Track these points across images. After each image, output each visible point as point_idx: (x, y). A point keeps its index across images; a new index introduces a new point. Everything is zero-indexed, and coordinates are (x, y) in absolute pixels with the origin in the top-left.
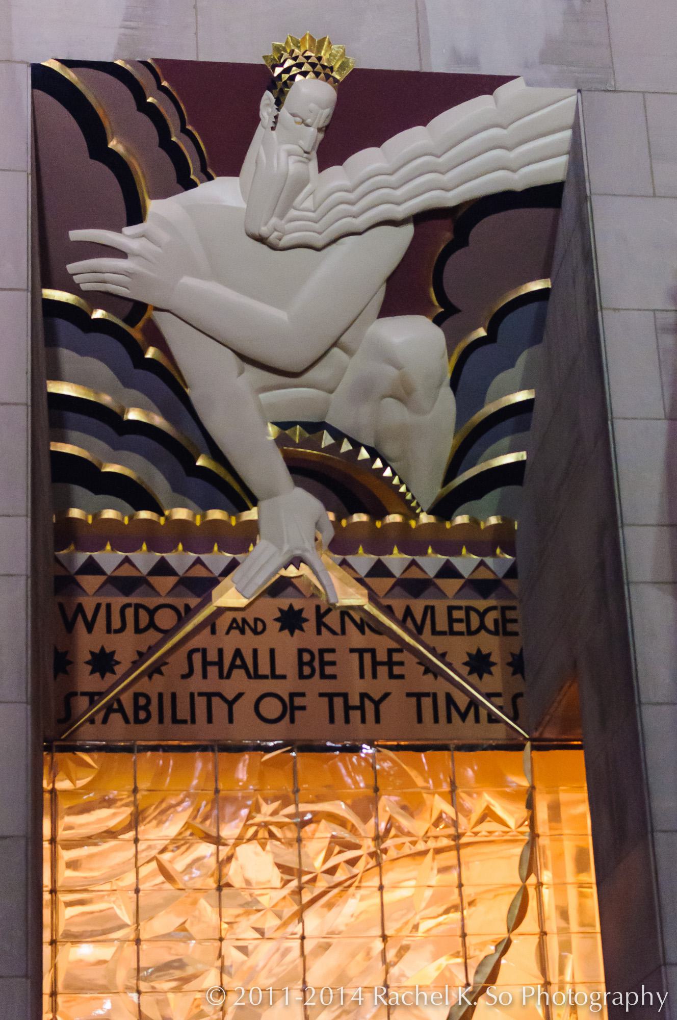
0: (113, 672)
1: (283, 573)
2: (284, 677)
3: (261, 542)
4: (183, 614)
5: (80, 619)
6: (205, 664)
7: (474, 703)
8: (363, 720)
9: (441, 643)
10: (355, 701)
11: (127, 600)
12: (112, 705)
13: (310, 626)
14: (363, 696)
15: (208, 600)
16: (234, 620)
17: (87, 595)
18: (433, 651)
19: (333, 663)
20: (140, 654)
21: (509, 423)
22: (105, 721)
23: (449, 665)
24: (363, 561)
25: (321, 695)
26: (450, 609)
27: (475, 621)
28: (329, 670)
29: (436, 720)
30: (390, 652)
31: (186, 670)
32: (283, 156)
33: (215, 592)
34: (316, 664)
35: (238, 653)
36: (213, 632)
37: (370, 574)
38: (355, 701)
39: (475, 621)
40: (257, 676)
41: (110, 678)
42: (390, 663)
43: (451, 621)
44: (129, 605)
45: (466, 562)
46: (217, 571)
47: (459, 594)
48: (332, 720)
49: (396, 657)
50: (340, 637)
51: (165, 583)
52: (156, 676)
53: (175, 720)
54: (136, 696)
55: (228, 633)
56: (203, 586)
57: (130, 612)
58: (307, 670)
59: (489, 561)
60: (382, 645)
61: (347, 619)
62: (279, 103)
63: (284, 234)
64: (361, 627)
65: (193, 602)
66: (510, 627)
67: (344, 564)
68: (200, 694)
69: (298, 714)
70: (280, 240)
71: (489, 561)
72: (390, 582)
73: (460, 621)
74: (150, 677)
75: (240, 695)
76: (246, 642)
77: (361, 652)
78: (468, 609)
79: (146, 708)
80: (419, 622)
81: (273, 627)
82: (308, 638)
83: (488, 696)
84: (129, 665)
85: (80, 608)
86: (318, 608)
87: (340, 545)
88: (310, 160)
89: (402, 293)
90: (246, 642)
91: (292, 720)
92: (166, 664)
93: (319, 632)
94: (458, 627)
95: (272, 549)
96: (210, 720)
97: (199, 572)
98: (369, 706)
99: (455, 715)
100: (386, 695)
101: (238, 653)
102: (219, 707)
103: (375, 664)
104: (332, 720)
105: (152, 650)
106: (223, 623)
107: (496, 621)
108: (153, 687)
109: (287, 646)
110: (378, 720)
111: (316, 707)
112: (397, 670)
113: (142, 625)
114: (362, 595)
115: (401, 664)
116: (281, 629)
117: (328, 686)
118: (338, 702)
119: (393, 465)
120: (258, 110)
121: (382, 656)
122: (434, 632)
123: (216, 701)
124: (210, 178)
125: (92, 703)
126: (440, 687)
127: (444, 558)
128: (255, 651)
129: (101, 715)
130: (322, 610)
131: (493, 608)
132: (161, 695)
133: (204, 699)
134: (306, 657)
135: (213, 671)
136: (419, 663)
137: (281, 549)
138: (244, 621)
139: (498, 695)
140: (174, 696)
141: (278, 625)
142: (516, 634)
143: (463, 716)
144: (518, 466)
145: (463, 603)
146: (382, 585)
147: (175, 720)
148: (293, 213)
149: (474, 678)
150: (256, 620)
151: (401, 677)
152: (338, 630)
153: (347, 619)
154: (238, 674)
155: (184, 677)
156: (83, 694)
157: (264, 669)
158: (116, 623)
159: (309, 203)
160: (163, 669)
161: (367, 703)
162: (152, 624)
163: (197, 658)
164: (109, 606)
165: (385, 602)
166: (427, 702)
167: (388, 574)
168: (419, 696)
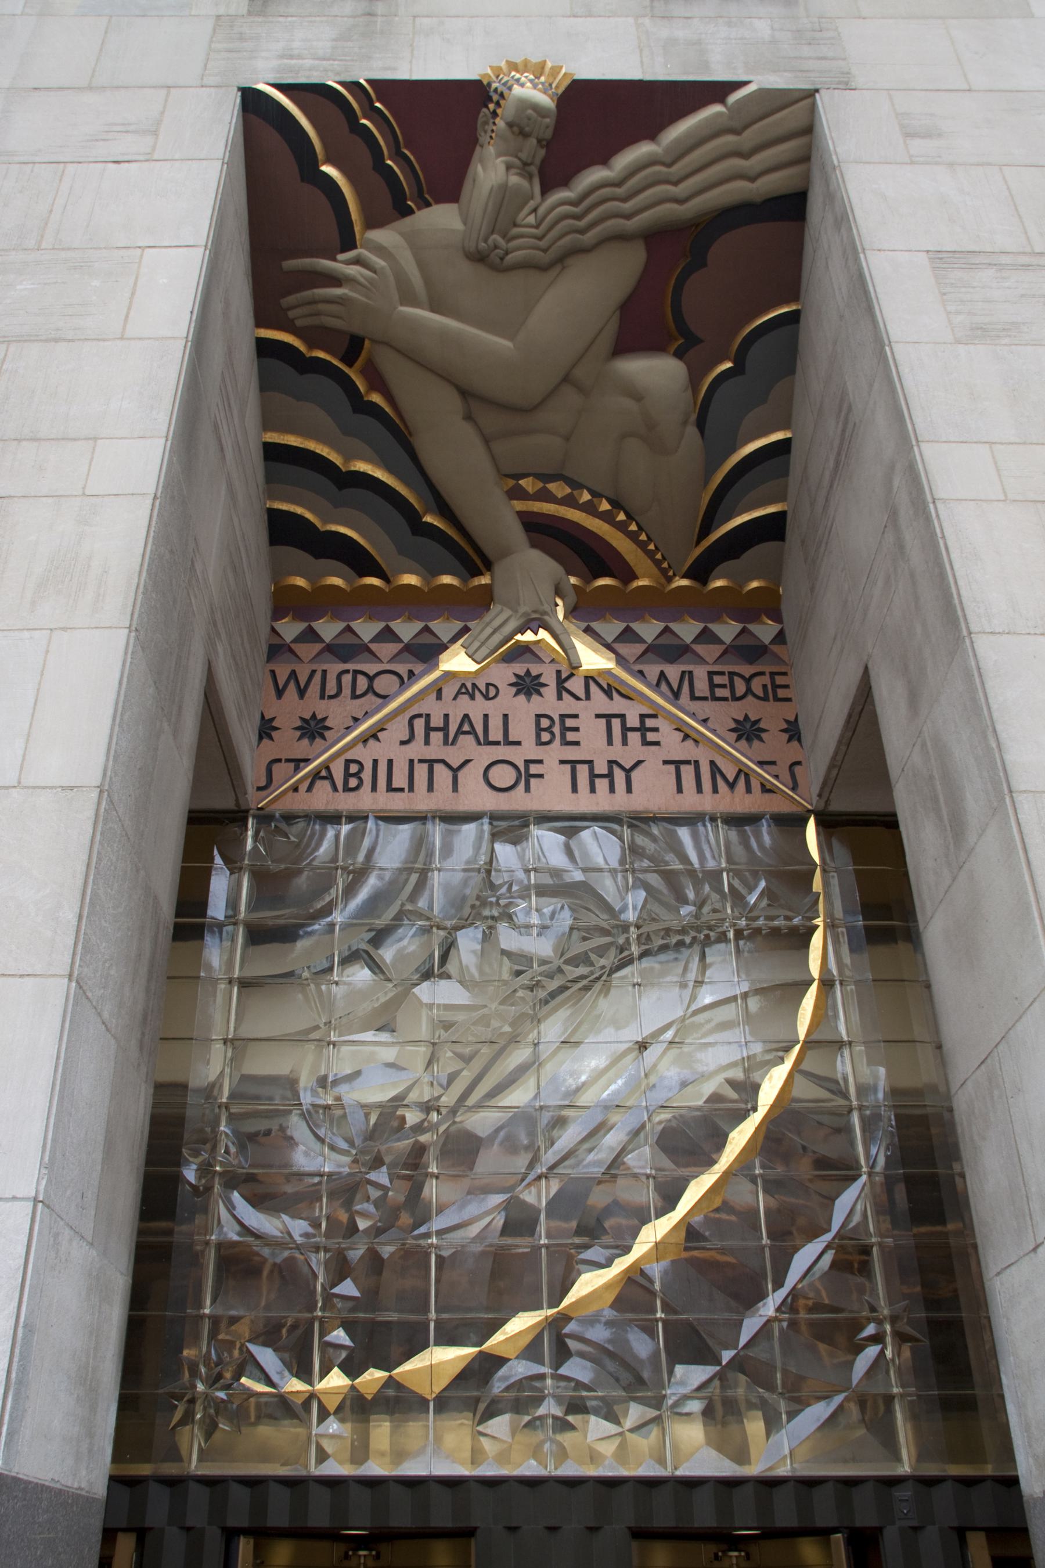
0: (324, 738)
2: (519, 743)
3: (495, 608)
4: (406, 680)
5: (292, 685)
6: (429, 729)
7: (742, 772)
8: (612, 789)
10: (601, 768)
12: (320, 772)
15: (437, 665)
16: (463, 685)
18: (693, 716)
19: (576, 729)
22: (309, 789)
23: (714, 731)
24: (611, 629)
25: (562, 762)
26: (711, 674)
27: (740, 687)
28: (571, 736)
29: (699, 789)
30: (643, 717)
32: (502, 168)
33: (443, 657)
34: (556, 730)
36: (439, 697)
37: (616, 640)
38: (601, 768)
39: (740, 687)
43: (712, 686)
44: (348, 671)
48: (575, 789)
49: (650, 723)
52: (371, 742)
53: (390, 789)
54: (348, 762)
55: (455, 699)
57: (347, 679)
58: (545, 737)
63: (507, 253)
64: (608, 692)
65: (418, 668)
67: (588, 630)
68: (421, 761)
69: (533, 781)
70: (502, 259)
72: (640, 648)
73: (723, 686)
74: (365, 741)
75: (467, 762)
77: (608, 717)
78: (732, 674)
79: (357, 775)
81: (507, 692)
82: (548, 702)
89: (641, 325)
90: (476, 708)
91: (527, 789)
92: (383, 729)
94: (720, 692)
95: (507, 613)
96: (430, 788)
98: (619, 776)
102: (442, 774)
103: (625, 729)
104: (575, 789)
105: (367, 715)
106: (449, 691)
107: (765, 686)
108: (365, 754)
109: (522, 713)
110: (629, 790)
111: (556, 777)
112: (651, 736)
113: (358, 692)
114: (609, 659)
115: (656, 730)
117: (572, 753)
118: (583, 771)
121: (633, 721)
122: (693, 697)
123: (438, 768)
124: (428, 205)
125: (297, 769)
128: (486, 716)
130: (564, 676)
131: (762, 674)
132: (375, 762)
133: (425, 766)
134: (545, 723)
135: (436, 737)
136: (677, 729)
137: (516, 611)
138: (474, 685)
139: (773, 763)
140: (390, 762)
141: (514, 690)
144: (781, 516)
146: (631, 651)
147: (390, 789)
148: (516, 231)
149: (743, 743)
150: (488, 685)
152: (582, 695)
154: (467, 740)
155: (403, 743)
158: (331, 688)
159: (531, 219)
160: (379, 734)
162: (370, 689)
163: (419, 724)
164: (324, 672)
165: (638, 667)
166: (687, 772)
168: (678, 764)
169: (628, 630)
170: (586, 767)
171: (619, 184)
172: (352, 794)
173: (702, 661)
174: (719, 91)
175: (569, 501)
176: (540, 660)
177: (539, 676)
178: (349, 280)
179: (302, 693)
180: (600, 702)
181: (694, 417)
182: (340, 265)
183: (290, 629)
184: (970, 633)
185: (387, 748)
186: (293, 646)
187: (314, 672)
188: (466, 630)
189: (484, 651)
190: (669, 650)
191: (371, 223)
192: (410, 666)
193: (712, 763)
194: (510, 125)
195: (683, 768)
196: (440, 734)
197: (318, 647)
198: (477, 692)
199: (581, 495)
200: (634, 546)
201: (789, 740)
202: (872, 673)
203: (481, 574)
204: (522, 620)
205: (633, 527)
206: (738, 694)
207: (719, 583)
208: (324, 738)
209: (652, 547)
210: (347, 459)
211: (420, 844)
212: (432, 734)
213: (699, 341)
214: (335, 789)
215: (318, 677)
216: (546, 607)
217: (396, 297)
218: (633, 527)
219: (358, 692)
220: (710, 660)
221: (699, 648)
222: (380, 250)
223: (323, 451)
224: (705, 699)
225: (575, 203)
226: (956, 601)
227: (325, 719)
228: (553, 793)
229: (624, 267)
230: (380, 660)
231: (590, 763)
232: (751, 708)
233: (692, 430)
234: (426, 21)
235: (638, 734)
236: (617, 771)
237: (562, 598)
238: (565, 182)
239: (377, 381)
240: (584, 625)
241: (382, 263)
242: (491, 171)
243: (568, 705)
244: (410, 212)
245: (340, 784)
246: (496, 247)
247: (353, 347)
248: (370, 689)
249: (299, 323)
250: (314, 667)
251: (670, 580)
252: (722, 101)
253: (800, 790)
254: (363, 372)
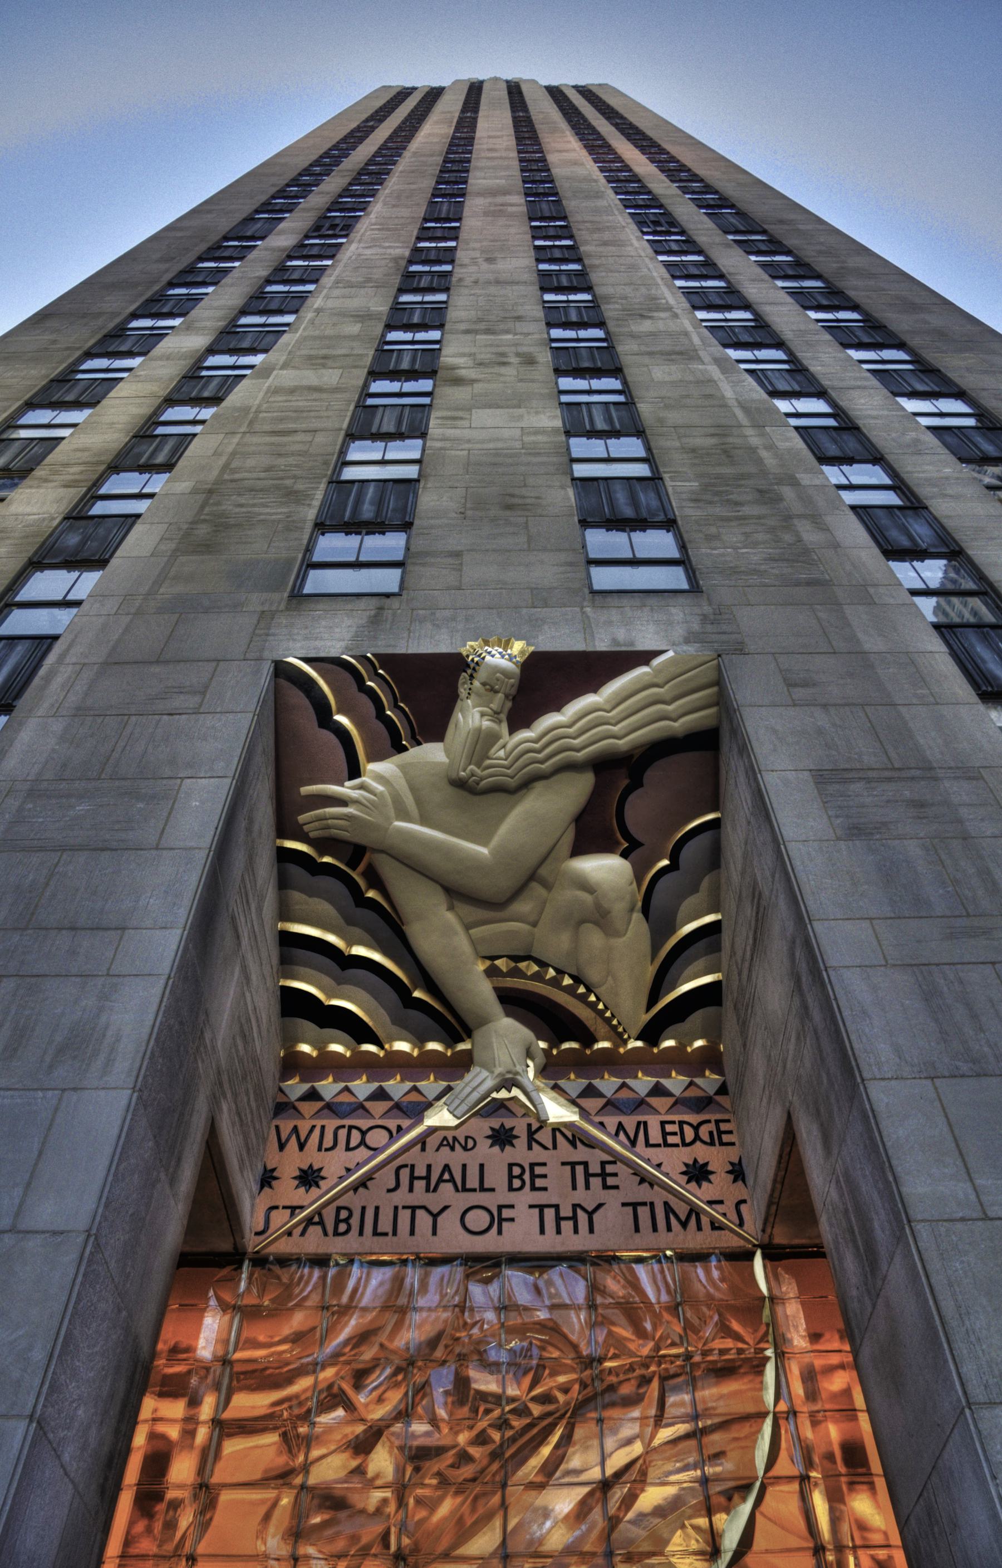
0: (318, 1186)
1: (494, 1095)
2: (493, 1190)
3: (475, 1070)
6: (413, 1178)
7: (694, 1212)
8: (576, 1231)
9: (658, 1154)
10: (566, 1211)
11: (340, 1122)
13: (521, 1143)
14: (575, 1207)
15: (421, 1121)
16: (445, 1138)
17: (304, 1118)
18: (648, 1161)
19: (545, 1176)
20: (348, 1170)
21: (701, 944)
22: (303, 1234)
23: (666, 1175)
24: (574, 1084)
25: (531, 1206)
26: (663, 1123)
28: (539, 1183)
29: (655, 1229)
30: (603, 1164)
31: (392, 1184)
34: (527, 1177)
35: (447, 1168)
36: (423, 1149)
37: (580, 1096)
38: (566, 1211)
39: (689, 1134)
40: (465, 1189)
41: (315, 1192)
42: (603, 1175)
43: (665, 1134)
44: (344, 1127)
45: (676, 1083)
46: (431, 1097)
47: (670, 1110)
48: (542, 1231)
49: (609, 1168)
50: (552, 1152)
51: (379, 1108)
52: (361, 1190)
53: (376, 1233)
54: (339, 1209)
55: (437, 1150)
56: (417, 1110)
57: (343, 1133)
59: (698, 1081)
60: (595, 1158)
61: (558, 1134)
62: (472, 677)
63: (482, 779)
65: (405, 1123)
66: (725, 1138)
67: (555, 1088)
69: (505, 1224)
71: (698, 1081)
72: (600, 1102)
73: (675, 1134)
74: (356, 1190)
76: (456, 1158)
77: (573, 1165)
78: (681, 1123)
79: (346, 1221)
80: (632, 1136)
82: (519, 1153)
83: (710, 1203)
84: (336, 1180)
85: (295, 1129)
86: (529, 1125)
87: (552, 1070)
88: (500, 721)
90: (456, 1158)
91: (500, 1232)
93: (530, 1148)
94: (671, 1139)
95: (485, 1074)
96: (412, 1232)
97: (414, 1097)
98: (582, 1217)
99: (673, 1221)
100: (600, 1206)
101: (447, 1168)
102: (423, 1219)
103: (588, 1175)
104: (542, 1231)
105: (359, 1166)
106: (433, 1141)
107: (711, 1133)
108: (354, 1201)
109: (498, 1161)
110: (591, 1230)
112: (610, 1181)
113: (352, 1145)
115: (615, 1175)
116: (491, 1146)
117: (540, 1198)
118: (549, 1214)
119: (597, 991)
120: (457, 688)
121: (595, 1168)
122: (648, 1144)
123: (420, 1214)
124: (419, 744)
125: (293, 1215)
126: (658, 1197)
127: (655, 1080)
128: (464, 1166)
129: (300, 1228)
130: (534, 1129)
131: (709, 1121)
132: (364, 1208)
133: (409, 1212)
134: (516, 1171)
135: (420, 1185)
137: (492, 1072)
138: (455, 1139)
140: (377, 1208)
142: (733, 1144)
143: (684, 1225)
144: (716, 985)
145: (676, 1118)
146: (592, 1104)
147: (376, 1233)
148: (488, 762)
149: (694, 1184)
151: (617, 1187)
152: (550, 1145)
153: (558, 1134)
154: (447, 1188)
155: (389, 1191)
156: (284, 1207)
157: (473, 1182)
158: (328, 1142)
159: (502, 753)
160: (369, 1183)
161: (579, 1211)
163: (405, 1174)
164: (323, 1127)
166: (644, 1212)
167: (600, 1095)
168: (635, 1205)
169: (590, 1085)
170: (552, 1210)
171: (570, 726)
172: (340, 1238)
173: (657, 1112)
174: (645, 657)
175: (538, 977)
176: (514, 1115)
177: (512, 1129)
178: (356, 802)
179: (302, 1146)
180: (565, 1151)
181: (640, 904)
182: (346, 789)
183: (295, 1087)
184: (863, 1080)
185: (375, 1196)
186: (297, 1104)
187: (314, 1127)
188: (449, 1089)
189: (464, 1107)
191: (373, 758)
192: (399, 1122)
193: (666, 1204)
194: (484, 684)
195: (640, 1209)
196: (423, 1183)
197: (320, 1104)
198: (457, 1145)
199: (546, 972)
200: (593, 1015)
201: (735, 1181)
202: (794, 1118)
203: (462, 1040)
204: (498, 1080)
205: (592, 998)
206: (688, 1140)
207: (670, 1043)
208: (318, 1186)
209: (608, 1014)
210: (350, 944)
211: (398, 1282)
212: (416, 1182)
213: (640, 844)
214: (326, 1234)
215: (317, 1132)
216: (519, 1068)
217: (392, 813)
218: (592, 998)
219: (352, 1145)
220: (663, 1111)
221: (654, 1101)
222: (380, 778)
223: (331, 938)
224: (659, 1145)
225: (536, 741)
226: (850, 1053)
227: (321, 1169)
228: (522, 1234)
229: (577, 790)
230: (373, 1117)
231: (557, 1207)
232: (701, 1153)
233: (637, 916)
234: (421, 612)
235: (600, 1179)
236: (580, 1213)
237: (533, 1059)
238: (527, 724)
239: (375, 880)
240: (553, 1082)
241: (380, 788)
243: (538, 1154)
244: (405, 749)
245: (330, 1229)
246: (473, 775)
247: (356, 853)
248: (362, 1142)
249: (312, 835)
250: (313, 1122)
251: (625, 1042)
252: (647, 663)
253: (745, 1228)
254: (364, 874)
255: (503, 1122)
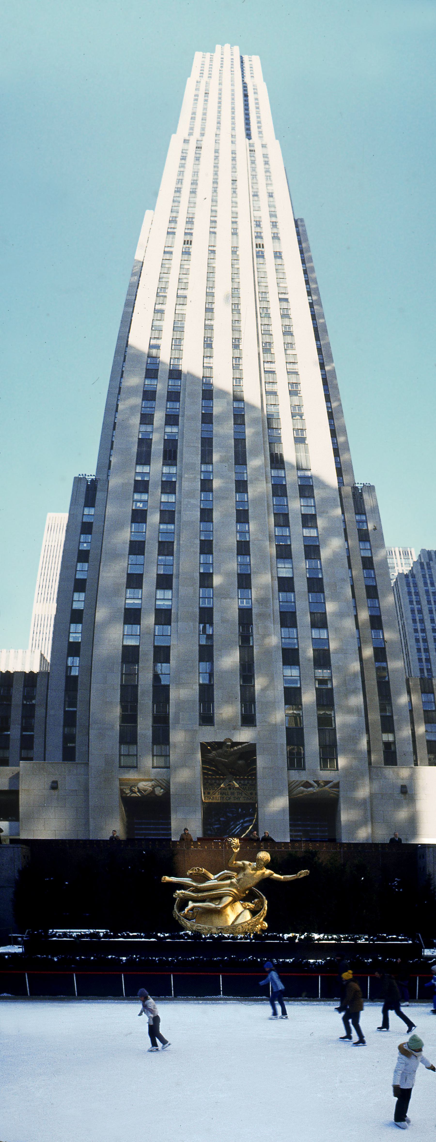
24: (238, 781)
45: (250, 782)
82: (232, 790)
87: (236, 780)
109: (229, 792)
190: (244, 785)
228: (232, 800)
242: (225, 748)
255: (231, 787)
